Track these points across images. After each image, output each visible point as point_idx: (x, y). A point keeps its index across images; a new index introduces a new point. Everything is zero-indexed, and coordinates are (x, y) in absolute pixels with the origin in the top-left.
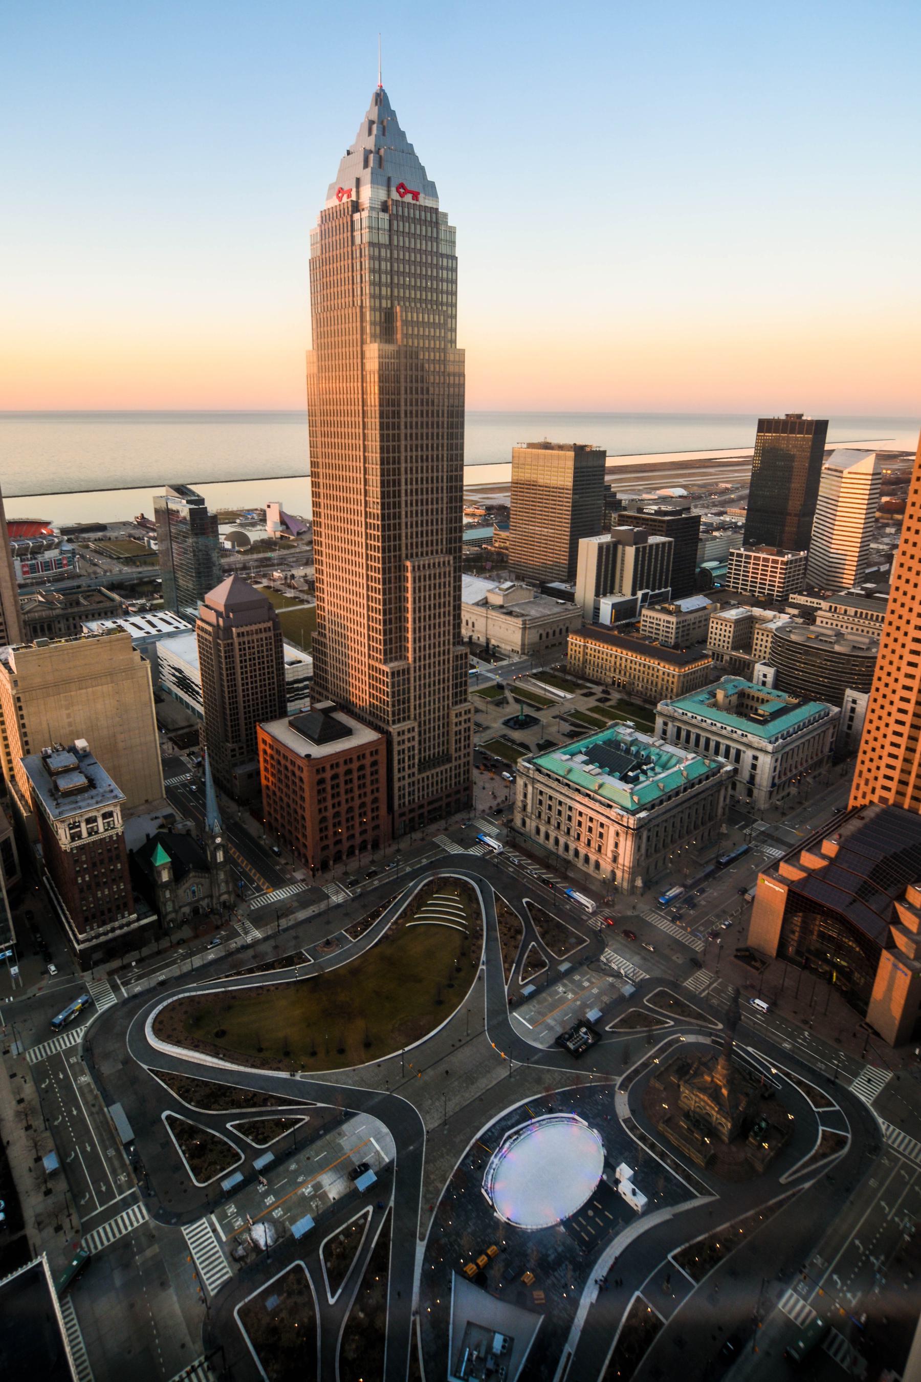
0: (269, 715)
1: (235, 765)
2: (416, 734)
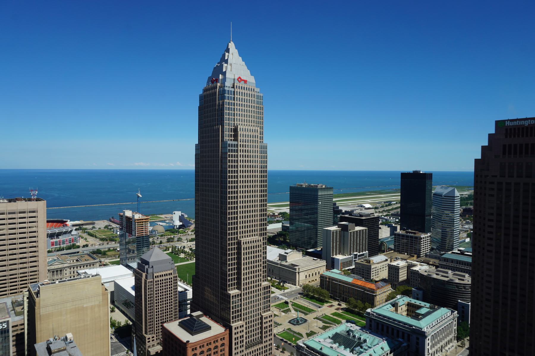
0: (169, 319)
1: (149, 347)
2: (244, 328)
